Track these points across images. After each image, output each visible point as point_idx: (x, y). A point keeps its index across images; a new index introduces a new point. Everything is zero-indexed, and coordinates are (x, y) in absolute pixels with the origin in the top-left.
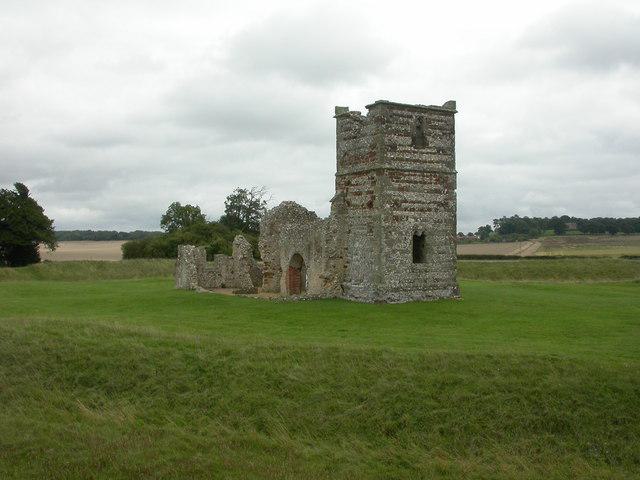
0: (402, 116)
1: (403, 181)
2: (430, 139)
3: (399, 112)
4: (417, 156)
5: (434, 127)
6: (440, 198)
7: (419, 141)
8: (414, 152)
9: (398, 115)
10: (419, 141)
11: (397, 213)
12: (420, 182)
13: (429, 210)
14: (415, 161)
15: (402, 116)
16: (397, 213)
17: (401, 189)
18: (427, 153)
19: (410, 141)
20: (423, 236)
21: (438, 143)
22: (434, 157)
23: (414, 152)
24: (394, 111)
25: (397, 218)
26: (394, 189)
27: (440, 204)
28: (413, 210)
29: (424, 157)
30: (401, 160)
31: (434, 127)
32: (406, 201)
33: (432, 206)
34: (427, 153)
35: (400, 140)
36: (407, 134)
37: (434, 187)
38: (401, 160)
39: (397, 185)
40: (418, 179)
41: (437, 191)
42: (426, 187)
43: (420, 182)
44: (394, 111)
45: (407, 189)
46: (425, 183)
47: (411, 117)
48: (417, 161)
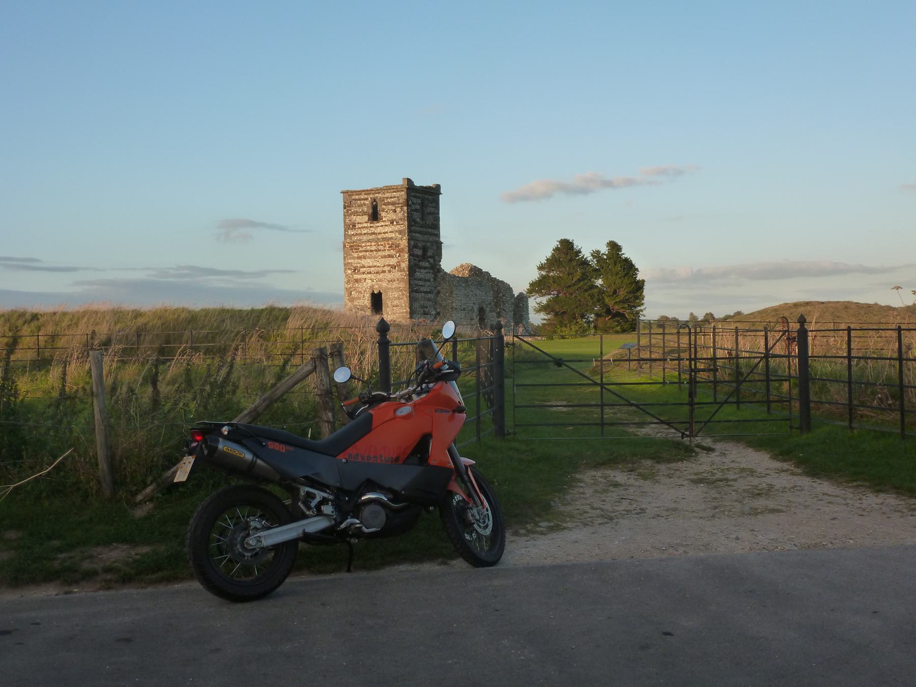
0: (360, 200)
1: (361, 252)
2: (383, 214)
3: (357, 197)
4: (373, 230)
5: (388, 204)
6: (393, 261)
7: (375, 216)
8: (371, 227)
9: (356, 200)
10: (375, 216)
11: (357, 276)
12: (376, 251)
13: (384, 272)
14: (373, 233)
15: (360, 200)
16: (357, 276)
17: (359, 258)
18: (382, 226)
19: (366, 218)
20: (380, 294)
21: (392, 216)
22: (387, 229)
23: (371, 227)
24: (353, 197)
25: (357, 281)
26: (354, 258)
27: (393, 267)
28: (370, 273)
29: (379, 230)
30: (361, 234)
31: (388, 204)
32: (364, 267)
33: (386, 269)
34: (382, 226)
35: (358, 219)
36: (364, 213)
37: (387, 253)
38: (361, 234)
39: (356, 255)
40: (373, 248)
41: (390, 256)
42: (380, 253)
43: (376, 251)
44: (353, 197)
45: (365, 257)
46: (380, 250)
47: (366, 199)
48: (373, 233)
